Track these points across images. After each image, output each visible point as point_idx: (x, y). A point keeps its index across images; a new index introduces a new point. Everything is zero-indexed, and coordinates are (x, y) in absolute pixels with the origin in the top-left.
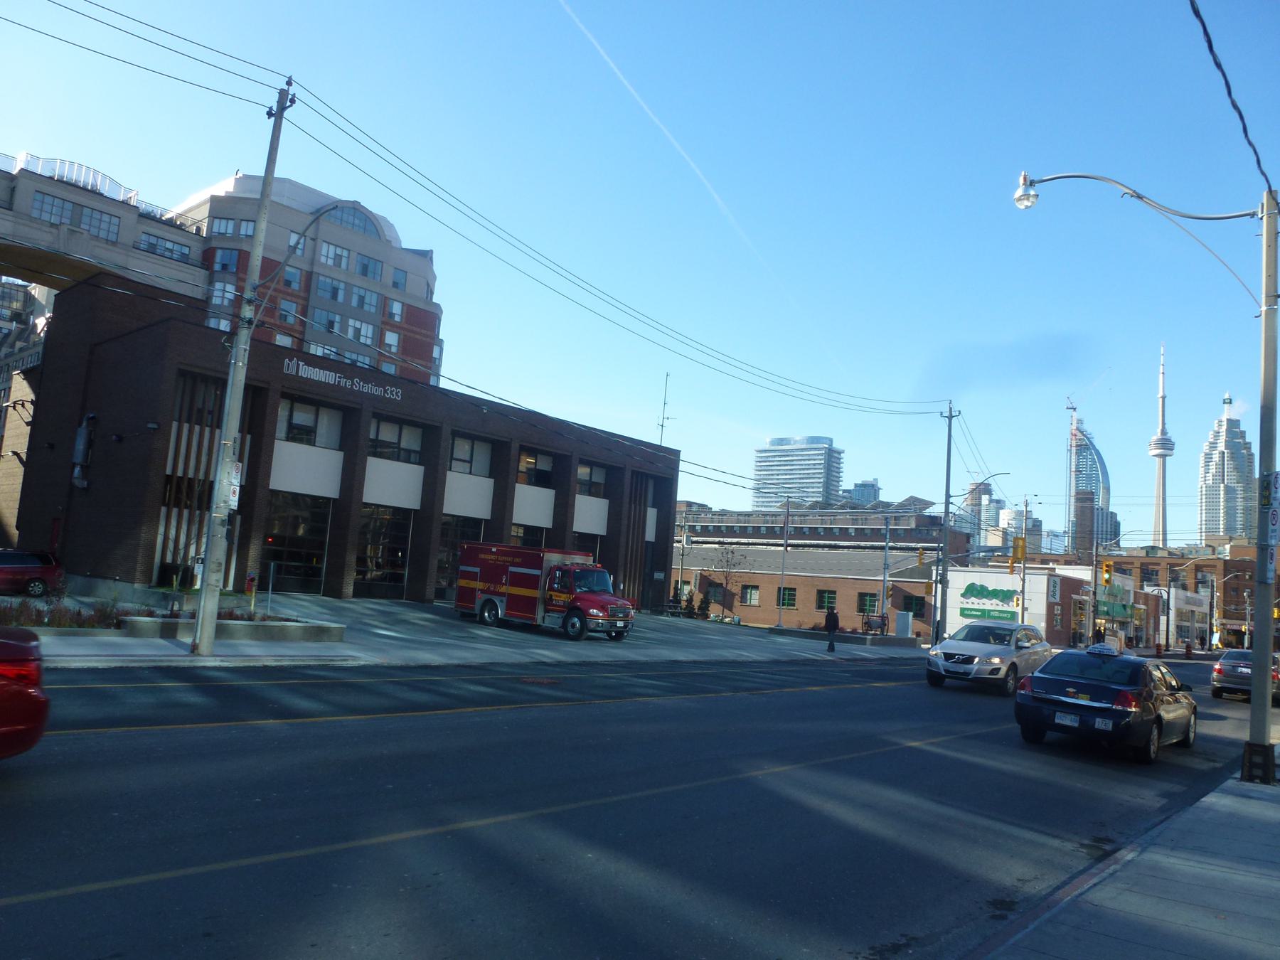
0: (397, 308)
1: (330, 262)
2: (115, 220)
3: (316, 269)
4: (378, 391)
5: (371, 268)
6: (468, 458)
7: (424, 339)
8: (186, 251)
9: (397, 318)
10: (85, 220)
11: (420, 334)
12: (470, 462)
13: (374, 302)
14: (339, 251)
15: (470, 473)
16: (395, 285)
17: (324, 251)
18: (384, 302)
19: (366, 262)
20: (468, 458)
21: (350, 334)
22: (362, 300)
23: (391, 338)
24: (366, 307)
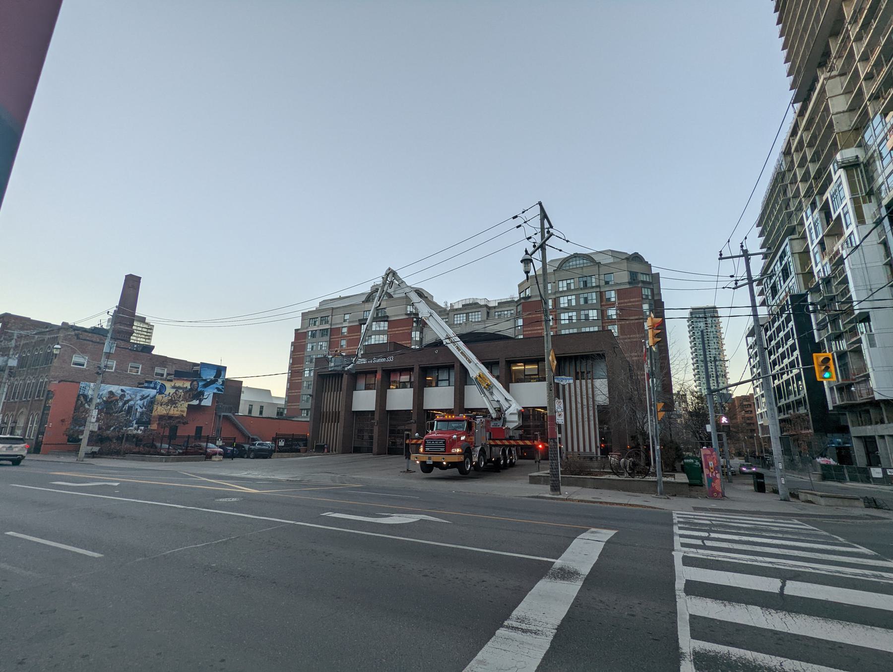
0: (613, 295)
1: (565, 289)
2: (479, 313)
3: (558, 295)
4: (384, 360)
5: (588, 282)
6: (448, 379)
7: (633, 304)
8: (512, 312)
9: (613, 300)
10: (470, 317)
11: (630, 302)
12: (449, 380)
13: (594, 297)
14: (569, 282)
15: (449, 386)
16: (607, 283)
17: (561, 285)
18: (601, 295)
19: (585, 279)
20: (448, 379)
21: (583, 317)
22: (586, 300)
23: (612, 312)
24: (590, 302)
